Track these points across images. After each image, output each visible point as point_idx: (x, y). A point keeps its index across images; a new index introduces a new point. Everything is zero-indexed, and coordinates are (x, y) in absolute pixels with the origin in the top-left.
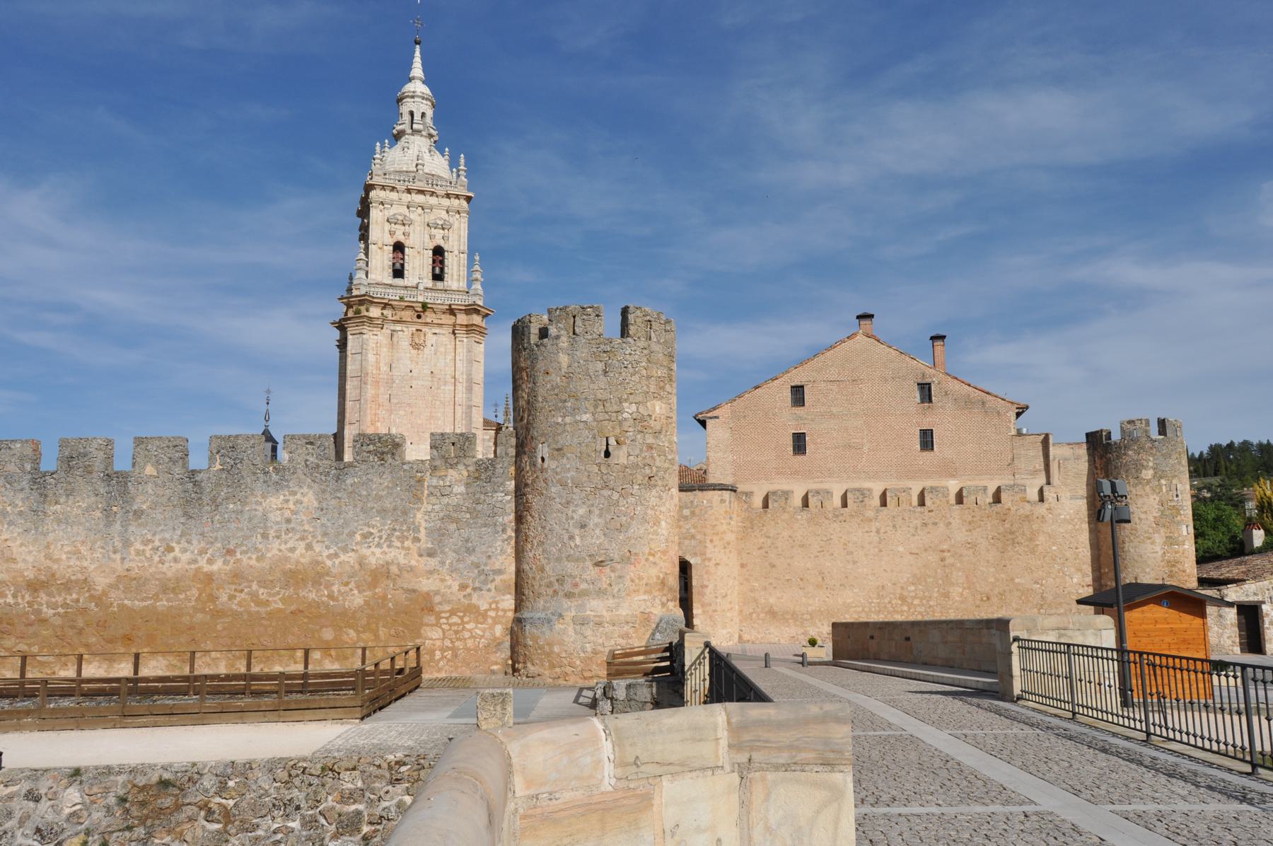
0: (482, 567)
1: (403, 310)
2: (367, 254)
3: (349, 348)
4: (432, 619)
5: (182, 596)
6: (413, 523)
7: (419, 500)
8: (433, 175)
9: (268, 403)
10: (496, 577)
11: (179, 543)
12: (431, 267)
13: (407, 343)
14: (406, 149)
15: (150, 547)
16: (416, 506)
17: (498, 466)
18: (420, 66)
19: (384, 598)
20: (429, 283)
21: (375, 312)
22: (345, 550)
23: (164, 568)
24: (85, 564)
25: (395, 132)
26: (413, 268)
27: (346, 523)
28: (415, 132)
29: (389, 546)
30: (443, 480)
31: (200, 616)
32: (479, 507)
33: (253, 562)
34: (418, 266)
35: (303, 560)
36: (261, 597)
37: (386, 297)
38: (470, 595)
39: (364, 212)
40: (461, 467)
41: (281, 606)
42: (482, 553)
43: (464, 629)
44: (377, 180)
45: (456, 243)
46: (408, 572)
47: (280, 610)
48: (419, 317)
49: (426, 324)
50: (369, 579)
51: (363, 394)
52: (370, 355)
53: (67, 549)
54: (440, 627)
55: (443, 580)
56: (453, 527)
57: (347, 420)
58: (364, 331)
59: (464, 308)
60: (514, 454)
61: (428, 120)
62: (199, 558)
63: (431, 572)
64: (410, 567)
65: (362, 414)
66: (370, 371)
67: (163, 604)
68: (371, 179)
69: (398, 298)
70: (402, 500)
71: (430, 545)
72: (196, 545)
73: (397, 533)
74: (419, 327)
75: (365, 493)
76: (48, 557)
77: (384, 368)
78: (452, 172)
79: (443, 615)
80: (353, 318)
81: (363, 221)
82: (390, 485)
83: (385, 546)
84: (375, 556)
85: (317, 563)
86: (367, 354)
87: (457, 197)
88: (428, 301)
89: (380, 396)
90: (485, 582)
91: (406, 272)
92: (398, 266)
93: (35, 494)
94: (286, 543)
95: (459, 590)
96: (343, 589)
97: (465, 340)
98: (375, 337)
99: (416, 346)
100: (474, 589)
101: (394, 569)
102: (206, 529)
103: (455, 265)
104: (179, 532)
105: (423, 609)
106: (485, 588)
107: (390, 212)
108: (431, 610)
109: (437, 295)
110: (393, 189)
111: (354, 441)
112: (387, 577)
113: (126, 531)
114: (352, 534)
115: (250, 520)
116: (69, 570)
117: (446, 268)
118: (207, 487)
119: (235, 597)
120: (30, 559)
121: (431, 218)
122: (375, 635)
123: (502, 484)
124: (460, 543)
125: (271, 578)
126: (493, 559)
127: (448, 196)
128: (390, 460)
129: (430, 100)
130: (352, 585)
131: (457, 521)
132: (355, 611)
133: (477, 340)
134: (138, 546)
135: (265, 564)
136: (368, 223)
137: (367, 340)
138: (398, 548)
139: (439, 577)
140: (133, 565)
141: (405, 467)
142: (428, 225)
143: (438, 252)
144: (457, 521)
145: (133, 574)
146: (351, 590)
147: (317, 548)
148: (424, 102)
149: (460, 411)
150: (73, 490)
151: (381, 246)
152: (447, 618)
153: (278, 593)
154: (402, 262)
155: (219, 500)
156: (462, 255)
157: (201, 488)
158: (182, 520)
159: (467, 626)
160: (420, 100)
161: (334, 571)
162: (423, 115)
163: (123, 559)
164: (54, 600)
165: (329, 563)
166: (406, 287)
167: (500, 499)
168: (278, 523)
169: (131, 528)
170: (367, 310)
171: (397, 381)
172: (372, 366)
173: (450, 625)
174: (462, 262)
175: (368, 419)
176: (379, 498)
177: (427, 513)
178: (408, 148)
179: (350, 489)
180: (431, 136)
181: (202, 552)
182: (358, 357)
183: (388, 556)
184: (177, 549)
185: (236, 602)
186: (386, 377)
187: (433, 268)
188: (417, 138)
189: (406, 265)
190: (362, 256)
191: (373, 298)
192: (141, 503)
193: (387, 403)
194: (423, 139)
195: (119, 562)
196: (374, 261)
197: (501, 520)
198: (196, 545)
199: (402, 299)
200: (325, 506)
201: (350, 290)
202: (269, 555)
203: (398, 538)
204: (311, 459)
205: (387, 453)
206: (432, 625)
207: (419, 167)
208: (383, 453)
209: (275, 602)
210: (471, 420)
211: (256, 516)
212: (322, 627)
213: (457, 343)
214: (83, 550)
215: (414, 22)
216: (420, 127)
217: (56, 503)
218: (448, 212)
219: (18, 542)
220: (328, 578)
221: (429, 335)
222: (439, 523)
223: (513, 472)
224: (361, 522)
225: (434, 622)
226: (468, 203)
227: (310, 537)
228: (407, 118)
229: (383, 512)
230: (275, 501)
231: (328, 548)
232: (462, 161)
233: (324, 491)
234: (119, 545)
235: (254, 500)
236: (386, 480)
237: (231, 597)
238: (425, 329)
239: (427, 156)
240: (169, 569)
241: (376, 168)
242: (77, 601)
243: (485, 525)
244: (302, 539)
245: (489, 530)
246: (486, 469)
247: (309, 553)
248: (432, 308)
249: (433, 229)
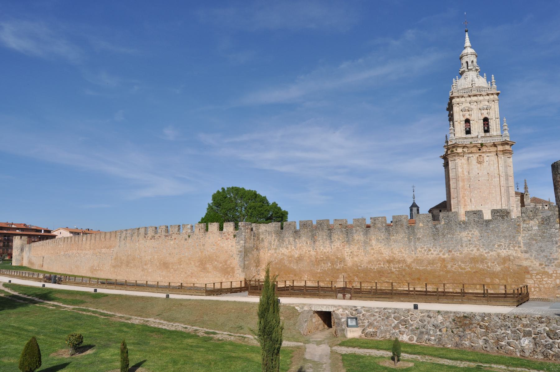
0: (549, 257)
2: (453, 126)
3: (450, 166)
4: (529, 276)
5: (435, 266)
6: (518, 241)
7: (519, 232)
8: (480, 87)
9: (414, 191)
10: (555, 261)
11: (432, 248)
12: (483, 127)
14: (466, 79)
15: (423, 249)
16: (518, 235)
17: (551, 219)
18: (468, 41)
19: (509, 268)
20: (483, 134)
21: (460, 150)
22: (492, 251)
23: (429, 256)
24: (404, 255)
25: (460, 72)
26: (475, 129)
27: (491, 241)
28: (469, 70)
29: (509, 249)
30: (528, 225)
31: (442, 273)
32: (545, 235)
33: (458, 255)
34: (477, 128)
35: (476, 254)
36: (462, 267)
37: (464, 143)
38: (544, 268)
39: (450, 108)
40: (535, 220)
41: (470, 270)
42: (548, 252)
43: (543, 280)
44: (455, 95)
45: (494, 115)
46: (517, 259)
47: (470, 271)
49: (483, 152)
50: (502, 261)
51: (458, 185)
52: (459, 169)
53: (398, 250)
54: (533, 279)
55: (532, 262)
56: (534, 242)
57: (452, 197)
58: (456, 159)
59: (501, 143)
60: (558, 214)
61: (475, 63)
62: (440, 253)
63: (527, 259)
64: (518, 257)
65: (458, 194)
66: (460, 176)
67: (429, 268)
68: (452, 94)
69: (469, 143)
70: (512, 232)
71: (525, 249)
72: (438, 249)
73: (512, 245)
74: (480, 154)
75: (497, 230)
76: (392, 253)
77: (466, 174)
78: (488, 83)
79: (533, 275)
80: (450, 154)
81: (450, 112)
82: (507, 227)
83: (507, 249)
84: (504, 253)
85: (482, 255)
86: (458, 168)
87: (492, 94)
88: (483, 142)
89: (465, 186)
90: (550, 263)
91: (471, 131)
92: (468, 129)
93: (387, 234)
94: (469, 248)
95: (539, 266)
96: (492, 264)
97: (503, 157)
98: (461, 161)
99: (479, 163)
100: (546, 265)
101: (512, 258)
102: (441, 244)
103: (494, 125)
104: (432, 245)
105: (525, 272)
106: (550, 265)
107: (462, 107)
108: (528, 273)
109: (487, 139)
110: (462, 97)
111: (491, 212)
112: (509, 260)
113: (415, 244)
114: (494, 245)
115: (456, 240)
116: (399, 257)
117: (490, 127)
118: (440, 230)
119: (453, 266)
120: (387, 253)
121: (481, 106)
122: (506, 281)
123: (554, 225)
124: (538, 248)
125: (465, 260)
126: (553, 254)
127: (488, 95)
128: (506, 218)
129: (475, 55)
130: (496, 263)
131: (536, 240)
132: (498, 273)
133: (508, 157)
134: (420, 249)
135: (463, 255)
136: (453, 113)
137: (458, 162)
138: (513, 250)
139: (530, 261)
140: (418, 255)
141: (512, 220)
142: (480, 109)
143: (486, 120)
144: (536, 240)
145: (419, 258)
146: (495, 265)
147: (481, 250)
148: (472, 56)
149: (503, 189)
150: (398, 232)
151: (459, 122)
152: (535, 276)
153: (468, 265)
154: (469, 127)
155: (445, 234)
156: (497, 120)
157: (438, 230)
158: (433, 241)
159: (544, 279)
160: (470, 56)
161: (489, 258)
162: (472, 62)
163: (415, 253)
164: (395, 266)
165: (486, 255)
166: (472, 138)
167: (553, 231)
168: (466, 241)
169: (417, 244)
170: (456, 150)
171: (472, 179)
172: (461, 173)
173: (537, 278)
174: (497, 123)
175: (461, 196)
176: (503, 232)
177: (523, 237)
178: (467, 78)
179: (492, 229)
180: (477, 70)
181: (441, 251)
182: (454, 170)
183: (509, 253)
184: (432, 250)
185: (454, 268)
186: (467, 177)
187: (484, 128)
188: (471, 72)
189: (471, 128)
190: (452, 128)
191: (458, 144)
192: (419, 235)
193: (469, 188)
194: (473, 72)
195: (414, 254)
196: (457, 129)
197: (555, 239)
198: (438, 249)
199: (471, 143)
200: (482, 235)
201: (447, 142)
202: (464, 252)
203: (512, 246)
204: (476, 219)
205: (505, 216)
206: (529, 278)
207: (473, 85)
208: (503, 216)
209: (468, 268)
211: (458, 239)
212: (485, 278)
213: (499, 159)
214: (403, 250)
215: (464, 23)
216: (472, 67)
217: (393, 236)
218: (488, 102)
219: (383, 248)
220: (486, 260)
221: (485, 157)
222: (528, 241)
223: (558, 221)
224: (497, 241)
225: (530, 277)
226: (498, 96)
227: (478, 246)
228: (465, 65)
229: (505, 237)
230: (464, 234)
231: (485, 250)
232: (493, 78)
233: (482, 230)
234: (413, 249)
235: (457, 233)
236: (505, 225)
237: (452, 267)
238: (483, 155)
239: (476, 79)
240: (430, 257)
241: (454, 89)
242: (402, 266)
243: (548, 241)
244: (475, 247)
245: (550, 243)
246: (546, 220)
247: (478, 252)
249: (482, 111)
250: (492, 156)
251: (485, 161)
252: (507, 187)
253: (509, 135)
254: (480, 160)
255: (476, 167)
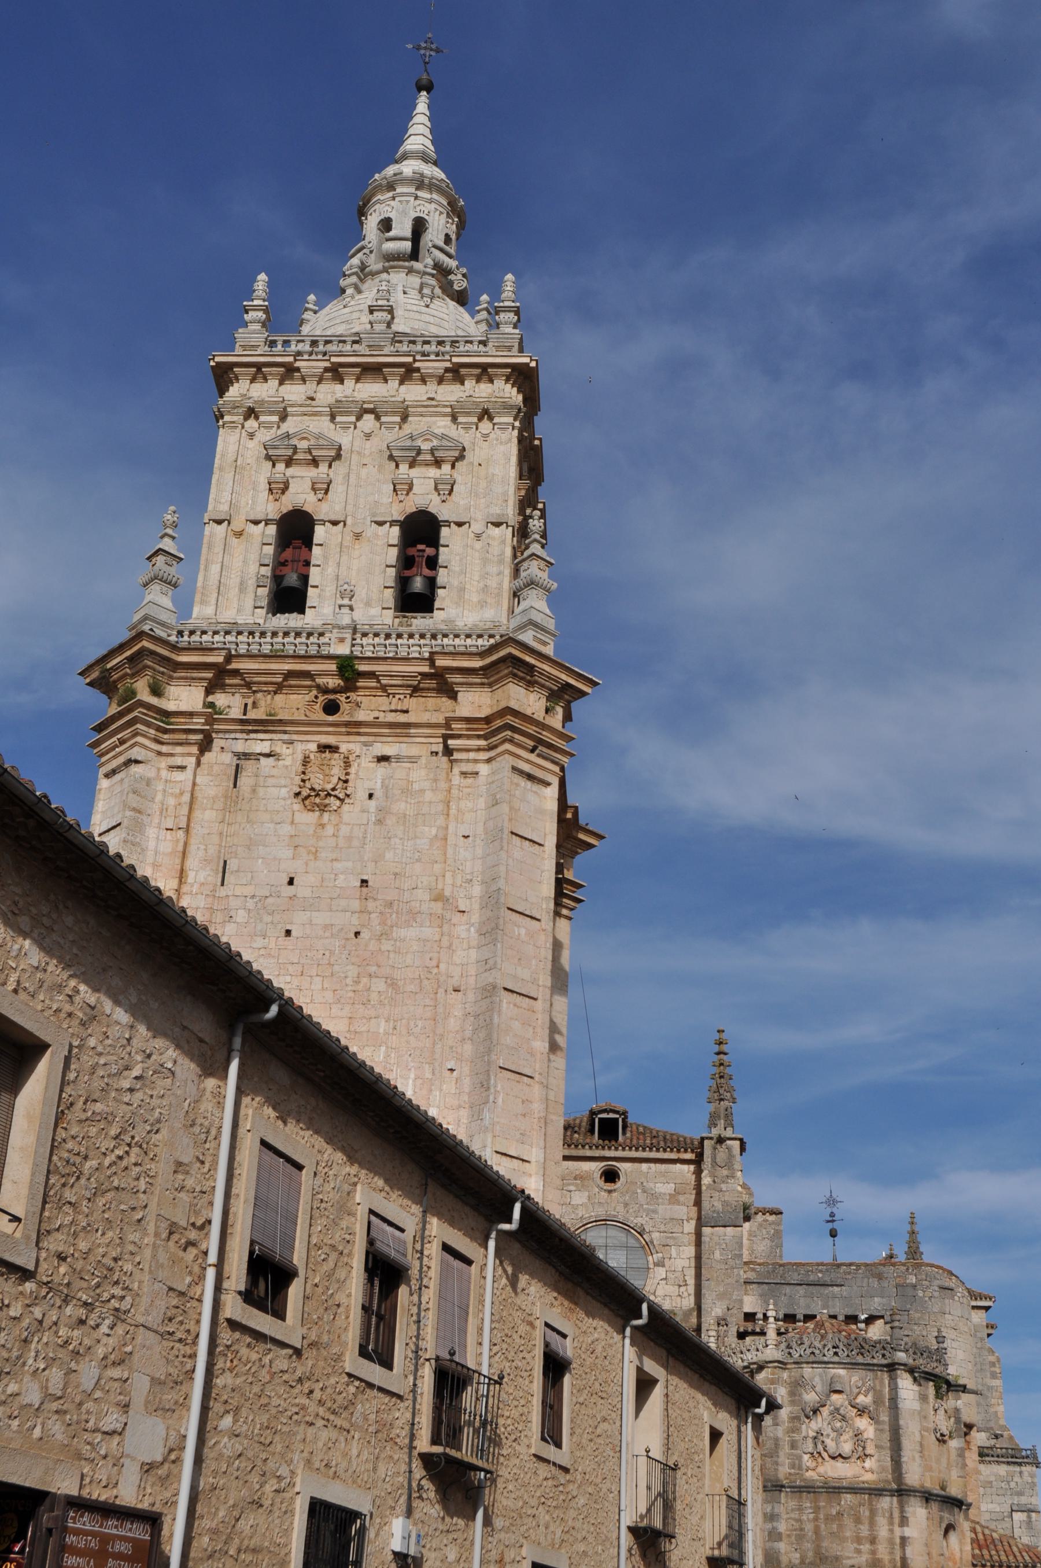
1: (279, 688)
13: (284, 792)
48: (331, 708)
49: (354, 727)
52: (151, 832)
58: (136, 753)
59: (477, 663)
74: (331, 740)
97: (484, 769)
98: (178, 776)
133: (526, 767)
171: (241, 916)
191: (174, 648)
210: (489, 1037)
248: (371, 675)
249: (404, 468)
250: (413, 760)
251: (359, 788)
252: (484, 989)
253: (550, 624)
254: (317, 780)
255: (286, 829)
